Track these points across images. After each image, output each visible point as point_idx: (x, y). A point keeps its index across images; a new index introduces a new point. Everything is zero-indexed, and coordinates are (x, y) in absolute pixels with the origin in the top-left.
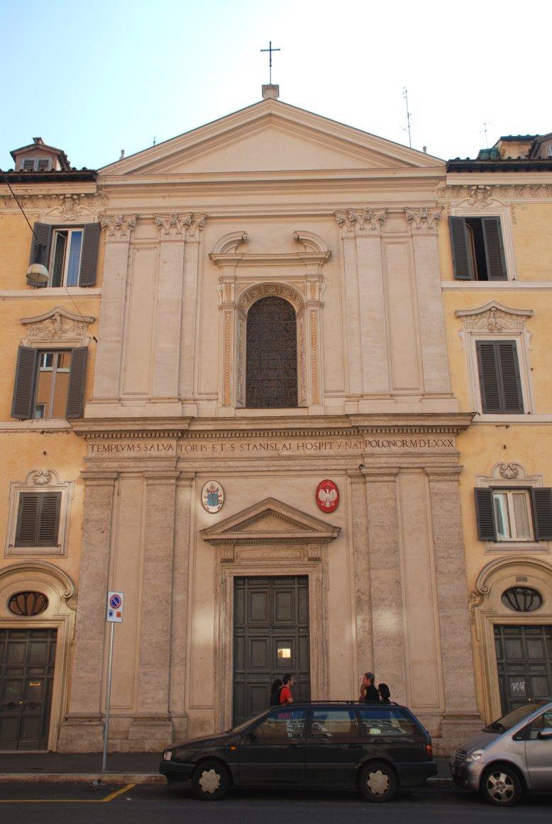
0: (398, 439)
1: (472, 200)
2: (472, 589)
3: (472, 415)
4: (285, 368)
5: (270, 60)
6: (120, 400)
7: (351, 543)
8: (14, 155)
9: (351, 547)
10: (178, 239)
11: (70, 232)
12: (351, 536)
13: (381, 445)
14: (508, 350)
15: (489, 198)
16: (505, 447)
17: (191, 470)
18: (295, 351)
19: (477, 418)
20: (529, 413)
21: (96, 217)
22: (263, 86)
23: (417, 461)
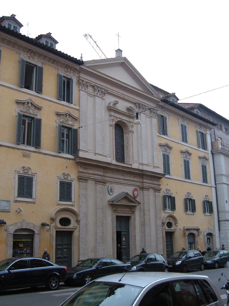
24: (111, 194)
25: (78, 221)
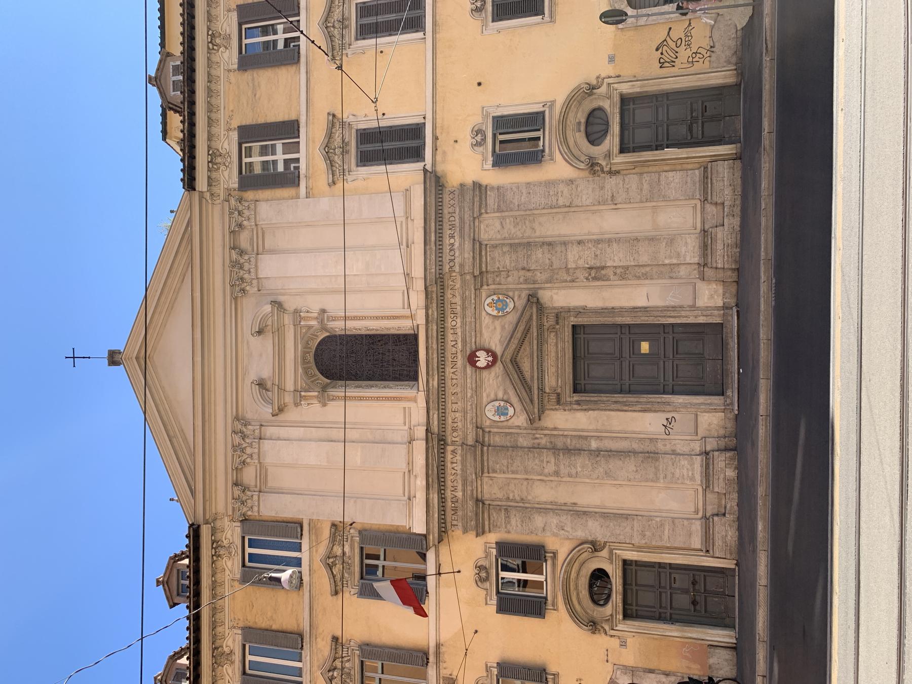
0: (447, 241)
1: (222, 168)
2: (586, 174)
3: (425, 171)
4: (382, 345)
5: (84, 358)
6: (409, 499)
7: (543, 286)
8: (173, 605)
9: (547, 285)
10: (257, 446)
11: (249, 550)
12: (537, 286)
13: (453, 258)
14: (365, 136)
15: (220, 150)
16: (456, 141)
17: (475, 432)
18: (366, 335)
19: (429, 167)
20: (424, 118)
21: (235, 524)
22: (109, 365)
23: (468, 224)
24: (511, 411)
25: (596, 547)
